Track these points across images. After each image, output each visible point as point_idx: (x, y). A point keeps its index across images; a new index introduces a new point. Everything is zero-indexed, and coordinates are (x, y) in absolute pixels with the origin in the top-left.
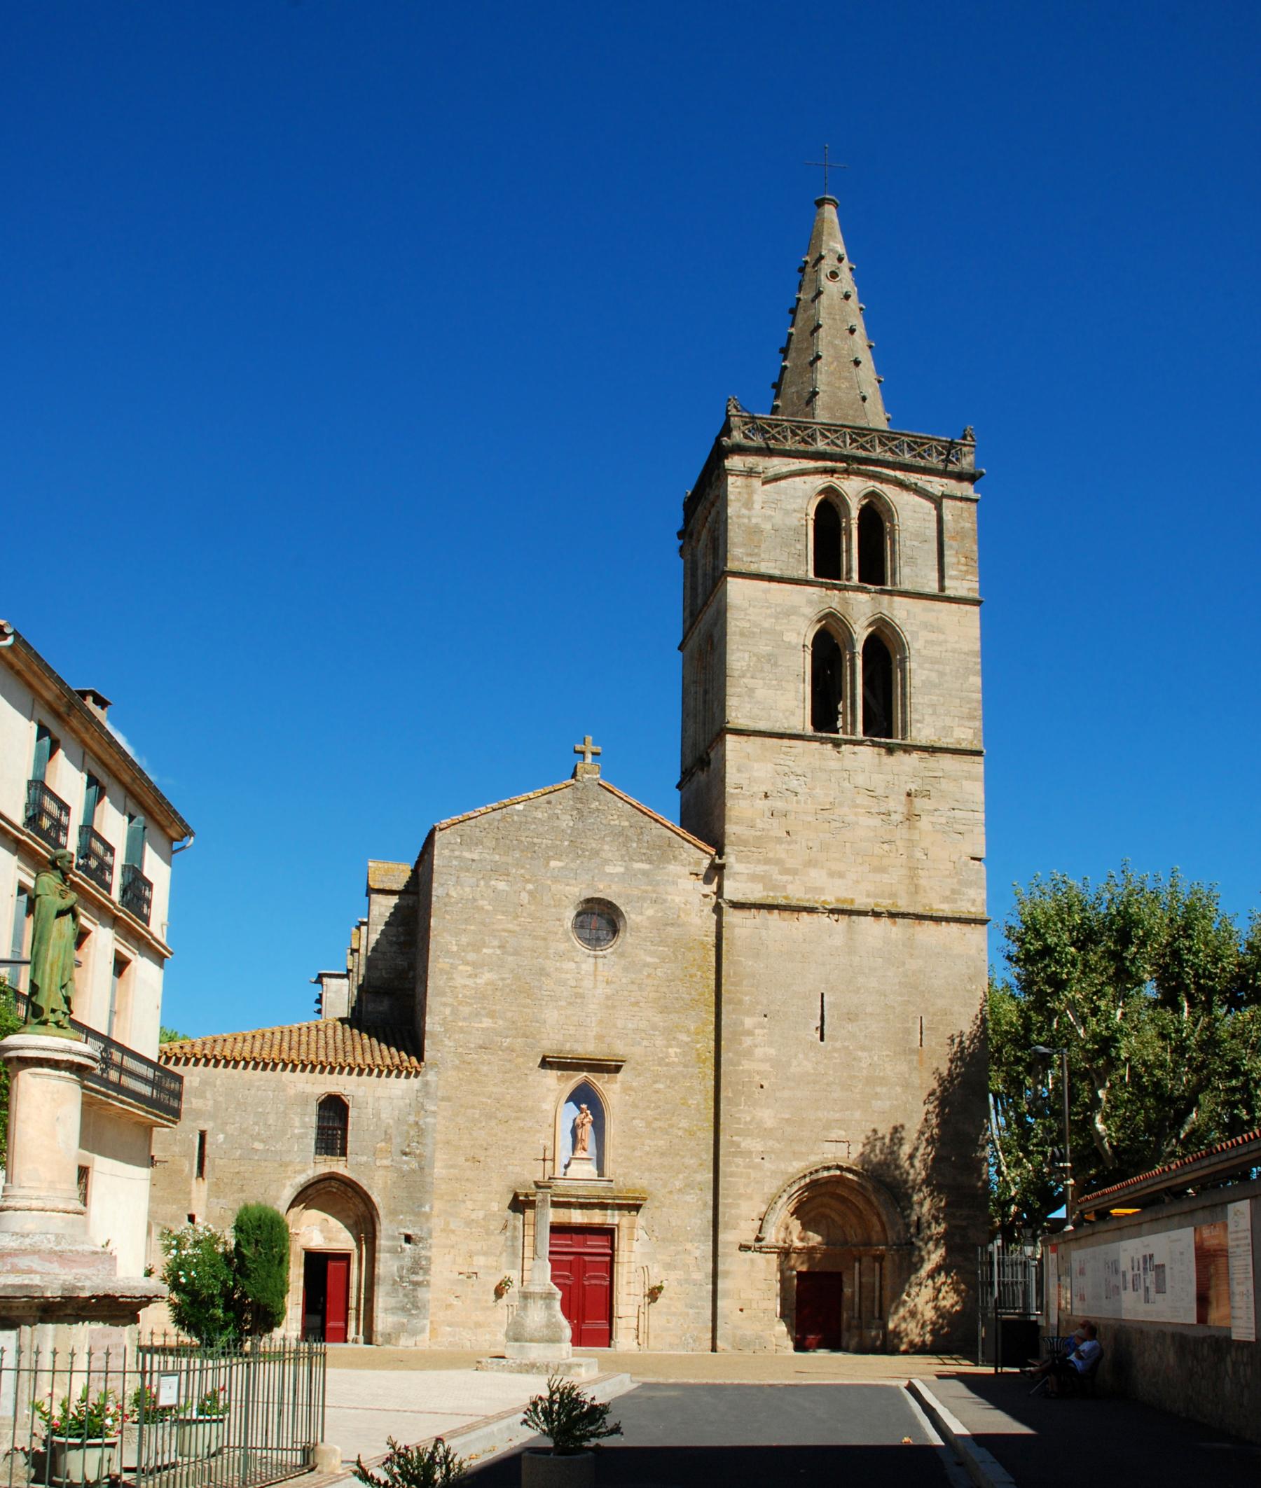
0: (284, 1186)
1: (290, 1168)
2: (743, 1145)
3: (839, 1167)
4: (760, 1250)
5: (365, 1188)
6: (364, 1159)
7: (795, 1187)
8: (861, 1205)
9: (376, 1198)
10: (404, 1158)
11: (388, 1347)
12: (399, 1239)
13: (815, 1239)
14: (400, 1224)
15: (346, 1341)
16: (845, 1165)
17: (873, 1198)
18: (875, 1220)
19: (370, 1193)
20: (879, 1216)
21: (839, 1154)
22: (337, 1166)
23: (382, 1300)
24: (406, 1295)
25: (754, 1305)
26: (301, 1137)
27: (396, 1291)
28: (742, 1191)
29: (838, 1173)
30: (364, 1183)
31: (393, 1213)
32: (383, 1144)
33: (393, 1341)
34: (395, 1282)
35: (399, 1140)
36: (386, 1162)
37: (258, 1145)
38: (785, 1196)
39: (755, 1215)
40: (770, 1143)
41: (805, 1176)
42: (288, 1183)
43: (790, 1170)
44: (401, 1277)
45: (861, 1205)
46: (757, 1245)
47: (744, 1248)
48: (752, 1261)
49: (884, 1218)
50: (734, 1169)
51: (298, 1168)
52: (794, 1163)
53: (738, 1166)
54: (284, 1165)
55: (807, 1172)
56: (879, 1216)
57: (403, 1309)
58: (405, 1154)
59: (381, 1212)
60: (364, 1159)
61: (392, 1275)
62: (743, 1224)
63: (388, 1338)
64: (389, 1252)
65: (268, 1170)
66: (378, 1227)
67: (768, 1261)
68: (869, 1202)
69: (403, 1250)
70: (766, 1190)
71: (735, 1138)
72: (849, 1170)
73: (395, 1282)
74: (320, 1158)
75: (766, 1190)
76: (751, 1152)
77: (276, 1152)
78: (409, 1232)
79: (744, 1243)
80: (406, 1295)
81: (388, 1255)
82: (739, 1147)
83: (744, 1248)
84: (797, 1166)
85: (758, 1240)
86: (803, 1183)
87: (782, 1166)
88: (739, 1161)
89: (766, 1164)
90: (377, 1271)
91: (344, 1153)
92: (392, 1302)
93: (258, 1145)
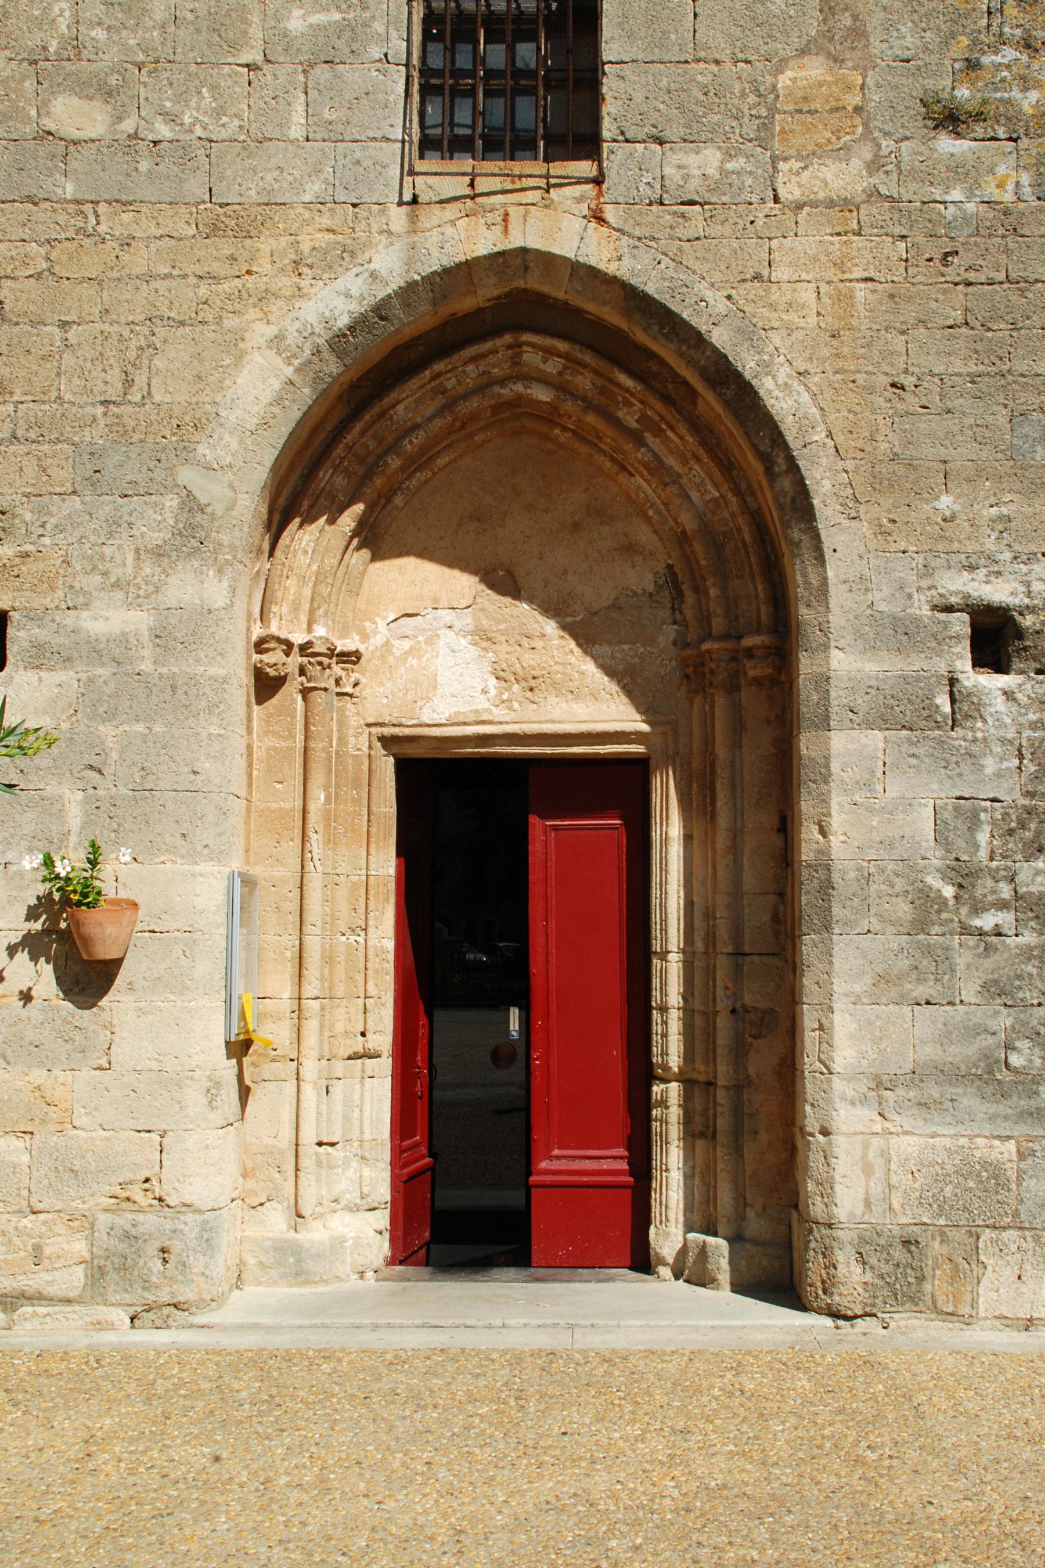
0: (235, 346)
1: (266, 245)
5: (720, 338)
6: (704, 162)
9: (787, 397)
10: (946, 144)
11: (910, 1330)
12: (942, 639)
14: (942, 542)
15: (643, 1262)
19: (747, 364)
22: (553, 219)
23: (858, 1024)
24: (996, 990)
26: (326, 55)
27: (942, 962)
30: (708, 305)
31: (896, 478)
32: (815, 69)
33: (936, 1285)
34: (926, 904)
35: (908, 38)
36: (841, 176)
37: (75, 115)
42: (261, 332)
44: (964, 876)
51: (310, 240)
54: (228, 223)
57: (990, 1076)
58: (950, 119)
59: (823, 481)
60: (704, 162)
61: (909, 867)
63: (908, 1270)
64: (882, 720)
65: (138, 261)
66: (801, 575)
69: (963, 706)
73: (926, 904)
74: (443, 177)
77: (183, 153)
78: (999, 592)
80: (996, 990)
81: (877, 737)
90: (809, 835)
91: (577, 137)
92: (916, 1035)
93: (75, 115)
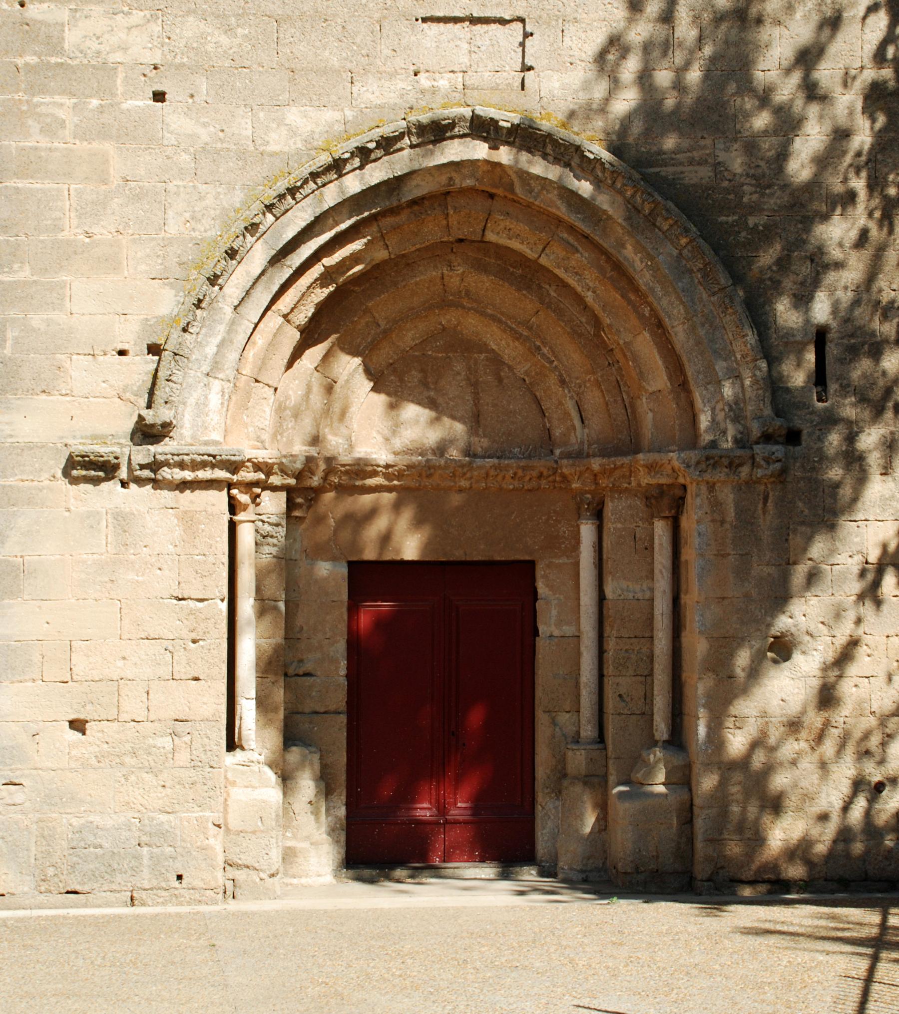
2: (71, 38)
3: (483, 128)
4: (152, 475)
7: (300, 216)
8: (590, 285)
13: (379, 430)
16: (507, 118)
17: (630, 254)
18: (645, 345)
20: (659, 329)
21: (483, 76)
25: (133, 706)
28: (71, 231)
29: (479, 150)
38: (258, 255)
39: (130, 334)
40: (191, 27)
41: (337, 167)
43: (278, 142)
45: (590, 285)
46: (143, 454)
47: (89, 468)
48: (122, 521)
49: (680, 334)
50: (36, 140)
52: (293, 115)
53: (52, 127)
55: (343, 149)
56: (659, 329)
62: (80, 372)
67: (188, 520)
68: (619, 274)
70: (173, 228)
71: (34, 11)
72: (526, 136)
75: (173, 228)
76: (107, 69)
79: (80, 447)
82: (54, 44)
83: (89, 468)
84: (306, 128)
85: (147, 433)
86: (331, 196)
87: (243, 127)
88: (59, 106)
89: (175, 118)
